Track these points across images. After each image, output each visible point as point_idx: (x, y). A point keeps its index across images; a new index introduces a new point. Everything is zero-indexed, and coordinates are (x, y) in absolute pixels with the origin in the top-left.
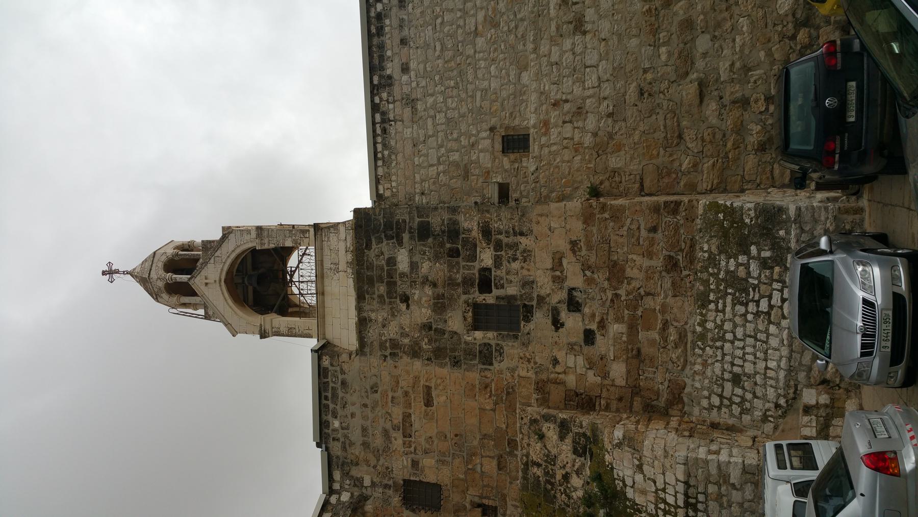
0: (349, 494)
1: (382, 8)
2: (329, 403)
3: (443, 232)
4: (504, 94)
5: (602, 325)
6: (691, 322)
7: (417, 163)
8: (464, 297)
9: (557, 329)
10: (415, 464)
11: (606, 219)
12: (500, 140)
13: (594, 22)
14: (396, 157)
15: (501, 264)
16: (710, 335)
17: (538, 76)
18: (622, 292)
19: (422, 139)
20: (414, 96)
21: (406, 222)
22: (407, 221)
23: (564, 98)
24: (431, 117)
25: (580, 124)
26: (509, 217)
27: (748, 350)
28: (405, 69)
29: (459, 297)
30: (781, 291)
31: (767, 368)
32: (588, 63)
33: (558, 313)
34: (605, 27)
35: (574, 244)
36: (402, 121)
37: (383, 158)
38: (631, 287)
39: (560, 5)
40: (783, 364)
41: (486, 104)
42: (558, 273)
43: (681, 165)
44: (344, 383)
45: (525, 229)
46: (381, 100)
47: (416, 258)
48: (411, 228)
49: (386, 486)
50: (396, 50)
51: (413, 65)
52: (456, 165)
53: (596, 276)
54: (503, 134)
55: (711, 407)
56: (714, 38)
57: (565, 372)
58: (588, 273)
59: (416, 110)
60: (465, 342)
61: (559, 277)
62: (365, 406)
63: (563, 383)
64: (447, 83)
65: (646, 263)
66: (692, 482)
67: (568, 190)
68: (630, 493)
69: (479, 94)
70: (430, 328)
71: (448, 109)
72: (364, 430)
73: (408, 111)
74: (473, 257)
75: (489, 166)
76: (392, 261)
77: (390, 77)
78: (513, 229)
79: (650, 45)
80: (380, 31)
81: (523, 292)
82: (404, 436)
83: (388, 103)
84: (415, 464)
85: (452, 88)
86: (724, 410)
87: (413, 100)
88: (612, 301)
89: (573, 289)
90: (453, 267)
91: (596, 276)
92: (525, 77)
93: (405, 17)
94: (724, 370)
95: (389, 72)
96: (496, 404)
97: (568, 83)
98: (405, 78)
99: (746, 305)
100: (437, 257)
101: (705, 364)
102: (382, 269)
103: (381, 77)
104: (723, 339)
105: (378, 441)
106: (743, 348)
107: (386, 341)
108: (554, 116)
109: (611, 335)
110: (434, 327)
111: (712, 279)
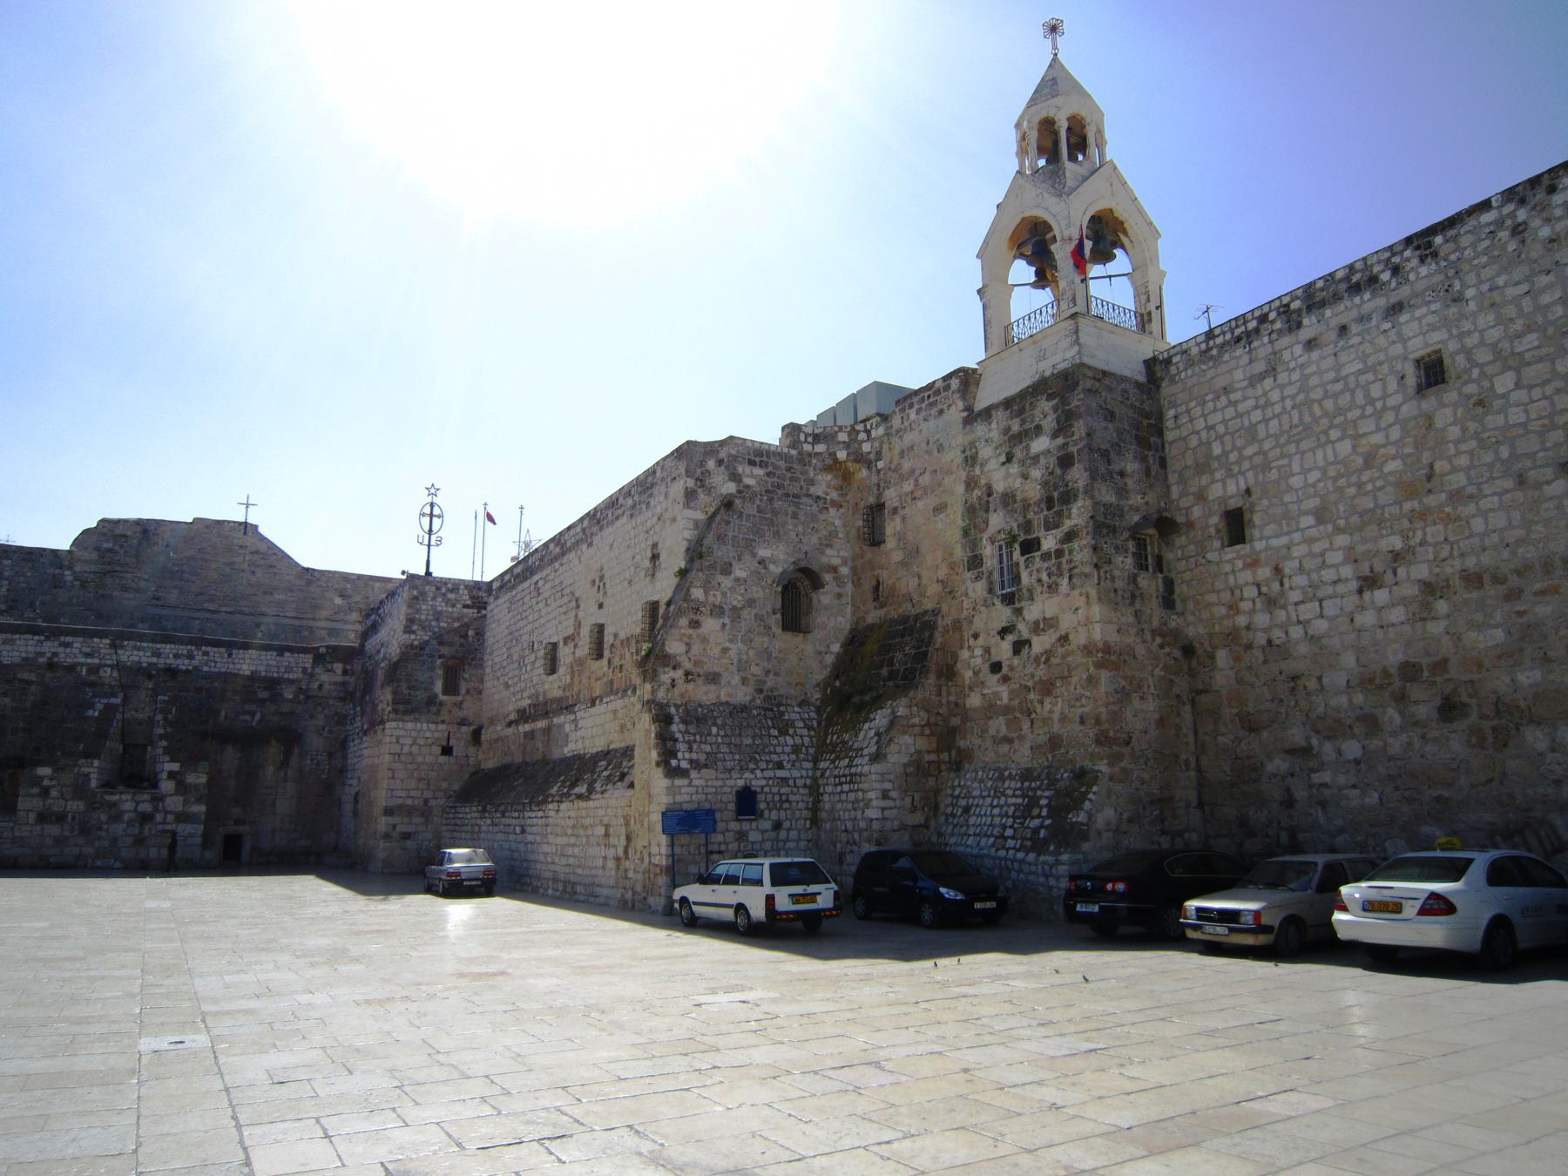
0: (869, 450)
1: (1385, 280)
2: (926, 402)
3: (1067, 485)
4: (1287, 498)
5: (1006, 679)
6: (1013, 765)
7: (1207, 398)
8: (1015, 525)
9: (999, 633)
10: (895, 510)
11: (1088, 671)
12: (1239, 506)
13: (1373, 602)
14: (1212, 367)
15: (1044, 561)
16: (1000, 784)
17: (1311, 541)
18: (1032, 696)
19: (1233, 397)
20: (1279, 370)
21: (1073, 435)
22: (1074, 438)
23: (1286, 580)
24: (1257, 402)
25: (1259, 606)
26: (1085, 560)
27: (984, 819)
28: (1310, 344)
29: (1016, 520)
30: (1014, 848)
31: (969, 835)
32: (1325, 604)
33: (1011, 632)
34: (1367, 619)
35: (1064, 639)
36: (1251, 361)
37: (1209, 349)
38: (1036, 704)
39: (1392, 552)
40: (969, 850)
41: (1274, 475)
42: (1042, 626)
43: (1222, 735)
44: (941, 412)
45: (1075, 580)
46: (1273, 322)
47: (1043, 461)
48: (1067, 444)
49: (878, 485)
50: (1334, 322)
51: (1315, 355)
52: (1209, 455)
53: (1042, 666)
54: (1244, 508)
55: (953, 788)
56: (1357, 762)
57: (969, 647)
58: (1043, 659)
59: (1264, 378)
60: (981, 539)
61: (1038, 628)
62: (928, 443)
63: (962, 648)
64: (1295, 414)
65: (1056, 717)
66: (863, 779)
67: (1191, 605)
68: (866, 726)
69: (1285, 462)
70: (989, 495)
71: (1267, 424)
72: (912, 447)
73: (1260, 367)
74: (1048, 528)
75: (1210, 498)
76: (1038, 430)
77: (1299, 325)
78: (1074, 567)
79: (1348, 681)
80: (1356, 289)
81: (1024, 591)
82: (912, 493)
83: (1270, 334)
84: (895, 510)
85: (1291, 422)
86: (950, 799)
87: (1274, 369)
88: (1026, 686)
89: (1030, 646)
90: (1039, 506)
91: (1042, 666)
92: (1308, 521)
93: (1374, 322)
94: (974, 798)
95: (1306, 321)
96: (942, 581)
97: (1301, 580)
98: (1298, 349)
99: (1013, 817)
100: (1045, 484)
101: (981, 781)
102: (1032, 421)
103: (1299, 311)
104: (995, 796)
105: (907, 465)
106: (985, 815)
107: (976, 447)
108: (1264, 573)
109: (1000, 689)
110: (991, 499)
111: (1038, 783)
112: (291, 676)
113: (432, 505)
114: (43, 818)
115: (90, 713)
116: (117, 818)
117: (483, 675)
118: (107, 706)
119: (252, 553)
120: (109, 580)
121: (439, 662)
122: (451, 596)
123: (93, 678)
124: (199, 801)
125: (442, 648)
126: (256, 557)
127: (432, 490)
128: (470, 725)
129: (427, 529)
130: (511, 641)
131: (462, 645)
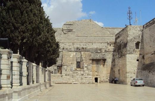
112: (104, 48)
113: (130, 11)
114: (66, 75)
115: (71, 56)
116: (78, 75)
117: (144, 45)
118: (73, 55)
119: (92, 25)
120: (69, 33)
121: (135, 43)
122: (136, 29)
123: (70, 50)
124: (91, 71)
125: (135, 40)
126: (93, 26)
127: (129, 8)
128: (142, 55)
129: (129, 16)
130: (151, 37)
131: (139, 39)
